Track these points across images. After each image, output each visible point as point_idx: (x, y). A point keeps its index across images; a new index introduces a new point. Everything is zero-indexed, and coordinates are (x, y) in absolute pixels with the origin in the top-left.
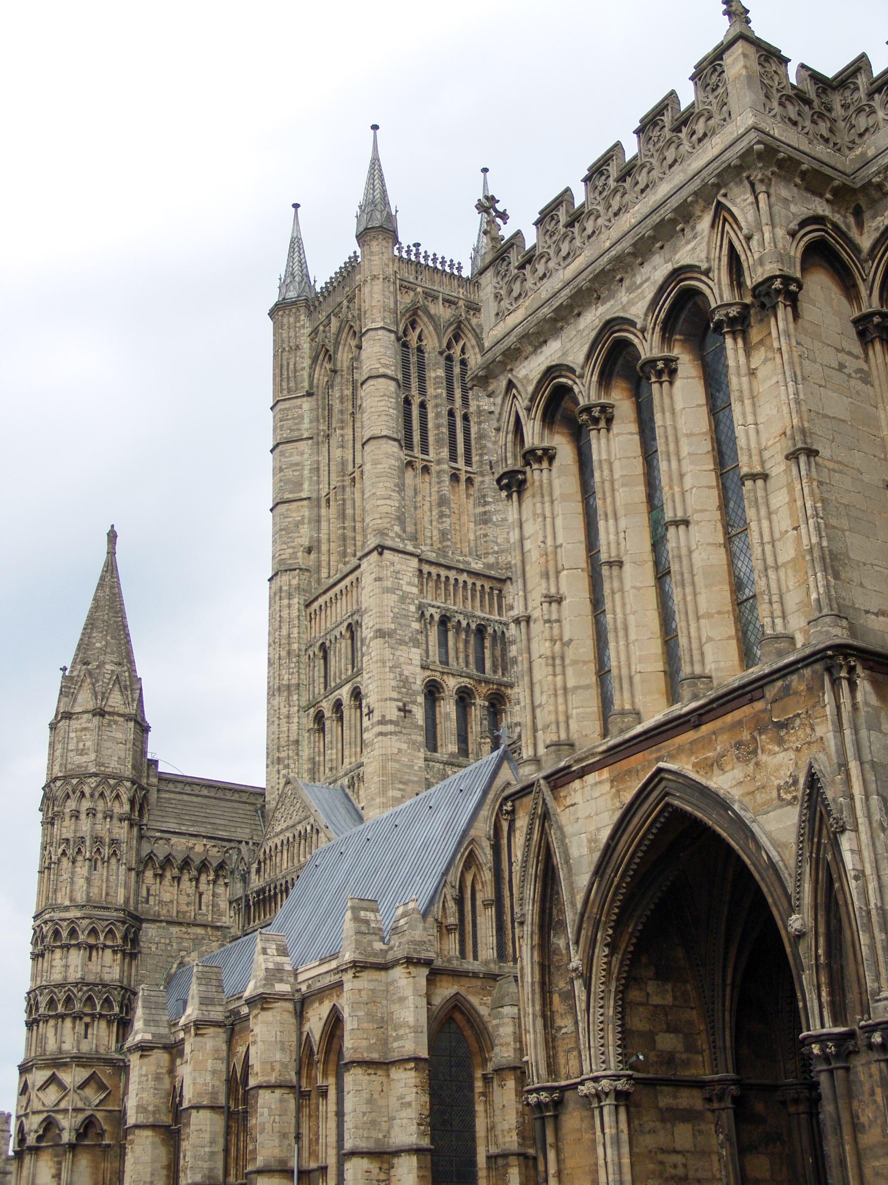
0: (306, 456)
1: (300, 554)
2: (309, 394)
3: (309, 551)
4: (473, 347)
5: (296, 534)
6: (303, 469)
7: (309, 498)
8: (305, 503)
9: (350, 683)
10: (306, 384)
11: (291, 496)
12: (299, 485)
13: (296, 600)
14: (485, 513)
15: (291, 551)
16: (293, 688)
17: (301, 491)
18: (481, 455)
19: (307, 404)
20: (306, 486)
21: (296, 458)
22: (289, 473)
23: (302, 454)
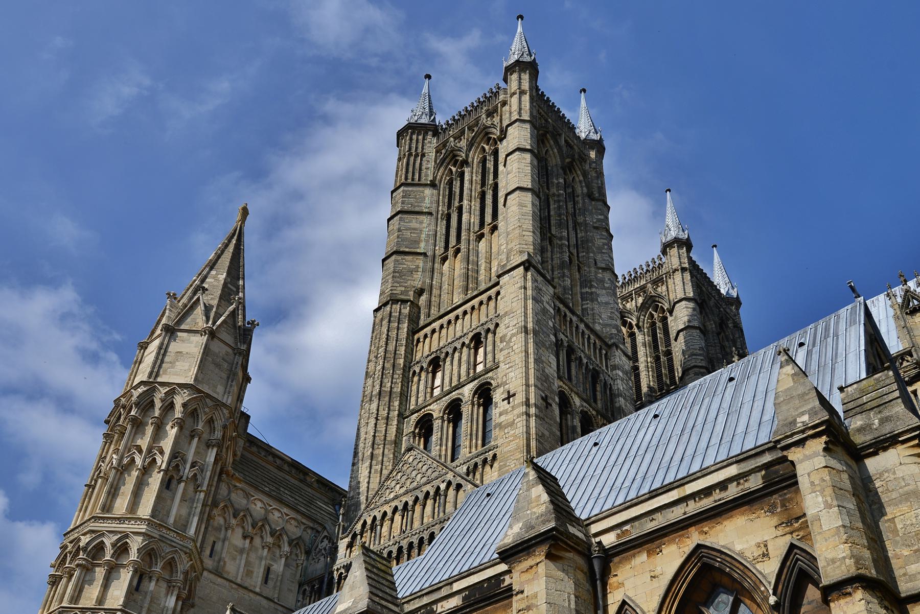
0: (425, 225)
1: (412, 293)
2: (433, 185)
3: (420, 292)
4: (580, 182)
5: (410, 278)
6: (421, 233)
7: (425, 254)
8: (421, 257)
9: (476, 381)
10: (431, 178)
11: (407, 250)
12: (417, 242)
13: (406, 325)
14: (592, 293)
15: (403, 289)
16: (394, 395)
17: (418, 248)
18: (588, 253)
19: (428, 191)
20: (422, 245)
21: (414, 225)
22: (408, 234)
23: (421, 223)
